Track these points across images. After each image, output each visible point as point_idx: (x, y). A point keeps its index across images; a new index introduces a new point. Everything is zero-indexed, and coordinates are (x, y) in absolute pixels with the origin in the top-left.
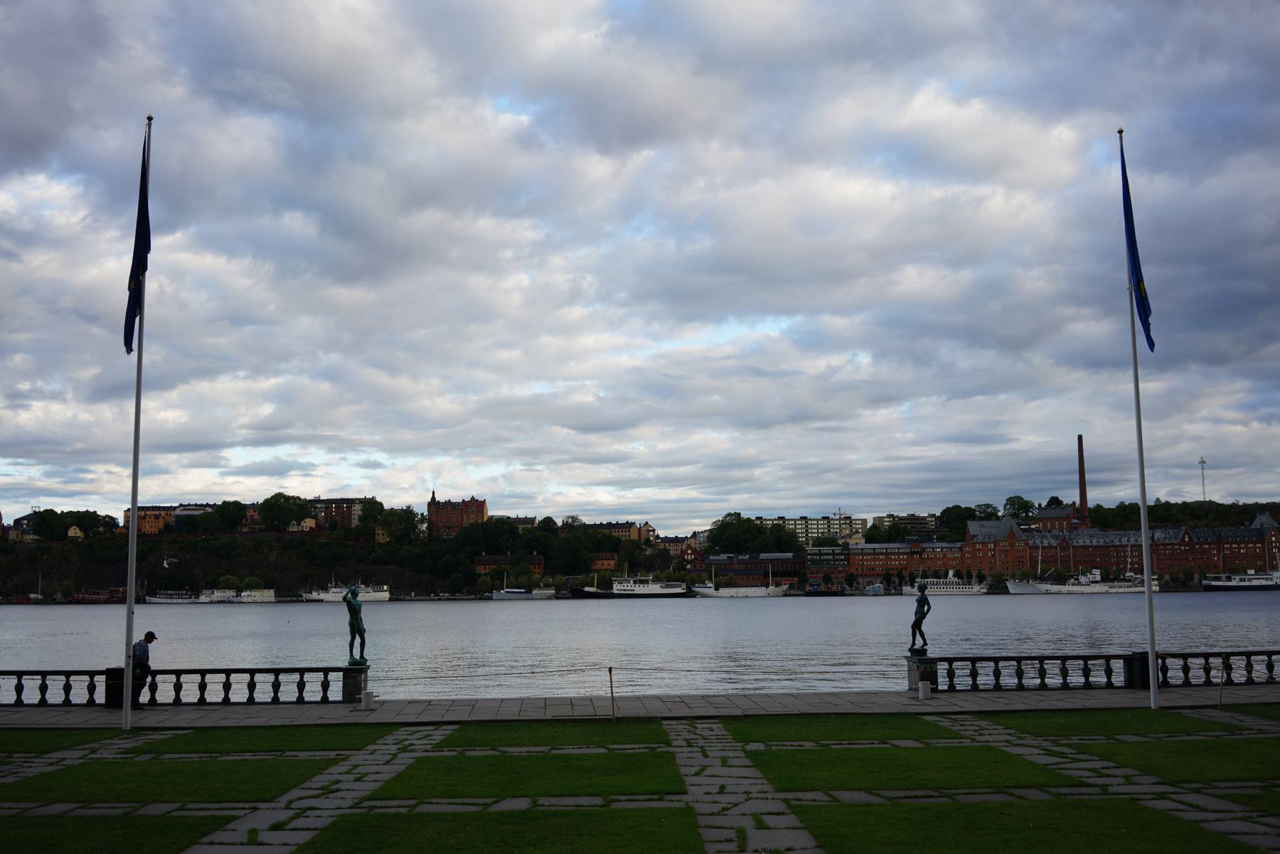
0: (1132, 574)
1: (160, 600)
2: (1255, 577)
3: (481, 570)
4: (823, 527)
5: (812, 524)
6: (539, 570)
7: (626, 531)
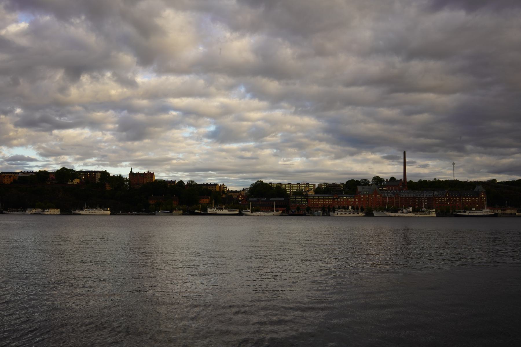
0: (425, 209)
1: (9, 213)
2: (475, 211)
3: (151, 202)
4: (297, 187)
5: (292, 186)
6: (176, 203)
7: (214, 187)
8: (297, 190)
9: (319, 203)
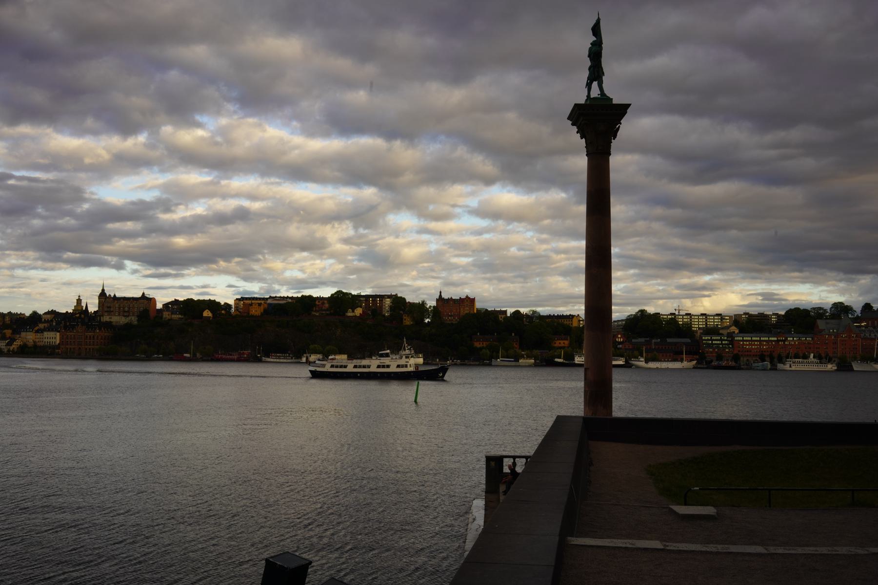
1: (272, 360)
5: (694, 319)
7: (569, 321)
8: (717, 325)
9: (753, 347)
